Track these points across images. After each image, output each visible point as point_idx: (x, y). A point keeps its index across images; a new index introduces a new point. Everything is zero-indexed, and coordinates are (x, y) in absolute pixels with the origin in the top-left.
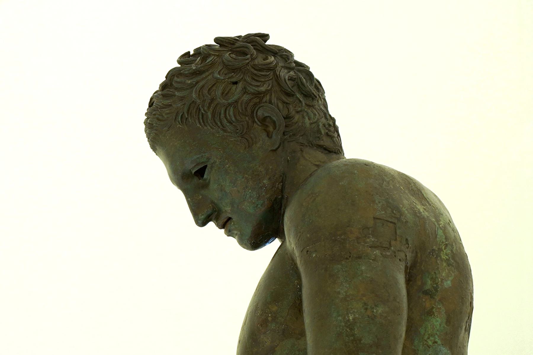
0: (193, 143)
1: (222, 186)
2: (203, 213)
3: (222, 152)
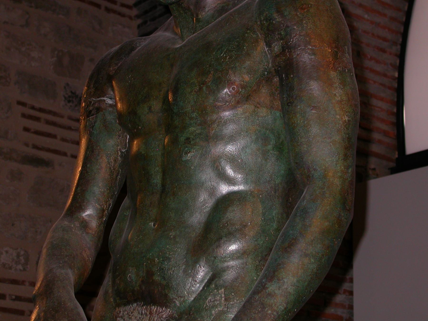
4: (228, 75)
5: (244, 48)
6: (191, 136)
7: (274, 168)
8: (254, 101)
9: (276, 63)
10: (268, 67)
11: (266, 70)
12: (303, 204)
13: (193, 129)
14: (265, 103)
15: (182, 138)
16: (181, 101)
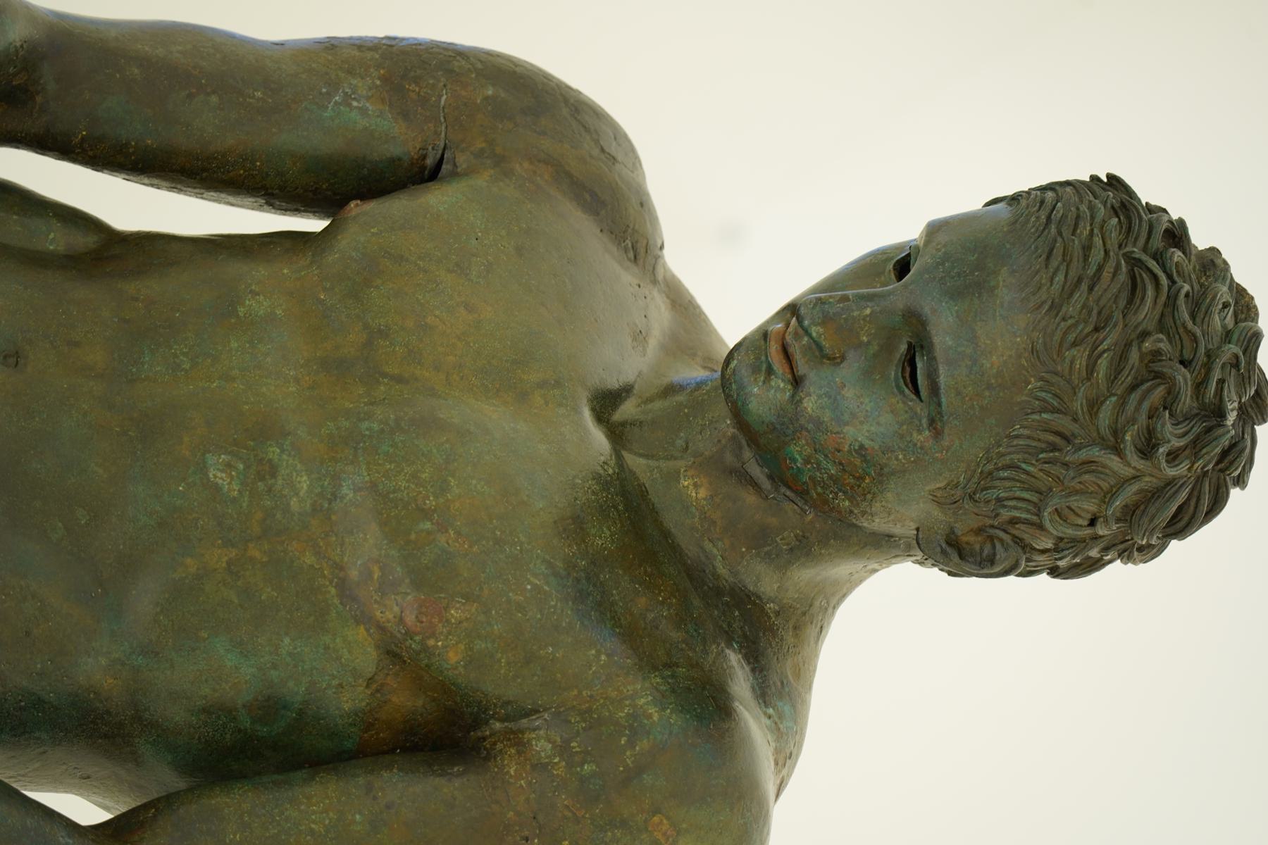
0: (977, 404)
1: (862, 423)
2: (823, 336)
3: (937, 455)
4: (464, 601)
5: (551, 649)
6: (280, 482)
7: (181, 734)
8: (388, 674)
9: (502, 742)
10: (492, 717)
11: (484, 713)
12: (62, 837)
13: (302, 487)
14: (381, 707)
15: (278, 451)
16: (392, 446)
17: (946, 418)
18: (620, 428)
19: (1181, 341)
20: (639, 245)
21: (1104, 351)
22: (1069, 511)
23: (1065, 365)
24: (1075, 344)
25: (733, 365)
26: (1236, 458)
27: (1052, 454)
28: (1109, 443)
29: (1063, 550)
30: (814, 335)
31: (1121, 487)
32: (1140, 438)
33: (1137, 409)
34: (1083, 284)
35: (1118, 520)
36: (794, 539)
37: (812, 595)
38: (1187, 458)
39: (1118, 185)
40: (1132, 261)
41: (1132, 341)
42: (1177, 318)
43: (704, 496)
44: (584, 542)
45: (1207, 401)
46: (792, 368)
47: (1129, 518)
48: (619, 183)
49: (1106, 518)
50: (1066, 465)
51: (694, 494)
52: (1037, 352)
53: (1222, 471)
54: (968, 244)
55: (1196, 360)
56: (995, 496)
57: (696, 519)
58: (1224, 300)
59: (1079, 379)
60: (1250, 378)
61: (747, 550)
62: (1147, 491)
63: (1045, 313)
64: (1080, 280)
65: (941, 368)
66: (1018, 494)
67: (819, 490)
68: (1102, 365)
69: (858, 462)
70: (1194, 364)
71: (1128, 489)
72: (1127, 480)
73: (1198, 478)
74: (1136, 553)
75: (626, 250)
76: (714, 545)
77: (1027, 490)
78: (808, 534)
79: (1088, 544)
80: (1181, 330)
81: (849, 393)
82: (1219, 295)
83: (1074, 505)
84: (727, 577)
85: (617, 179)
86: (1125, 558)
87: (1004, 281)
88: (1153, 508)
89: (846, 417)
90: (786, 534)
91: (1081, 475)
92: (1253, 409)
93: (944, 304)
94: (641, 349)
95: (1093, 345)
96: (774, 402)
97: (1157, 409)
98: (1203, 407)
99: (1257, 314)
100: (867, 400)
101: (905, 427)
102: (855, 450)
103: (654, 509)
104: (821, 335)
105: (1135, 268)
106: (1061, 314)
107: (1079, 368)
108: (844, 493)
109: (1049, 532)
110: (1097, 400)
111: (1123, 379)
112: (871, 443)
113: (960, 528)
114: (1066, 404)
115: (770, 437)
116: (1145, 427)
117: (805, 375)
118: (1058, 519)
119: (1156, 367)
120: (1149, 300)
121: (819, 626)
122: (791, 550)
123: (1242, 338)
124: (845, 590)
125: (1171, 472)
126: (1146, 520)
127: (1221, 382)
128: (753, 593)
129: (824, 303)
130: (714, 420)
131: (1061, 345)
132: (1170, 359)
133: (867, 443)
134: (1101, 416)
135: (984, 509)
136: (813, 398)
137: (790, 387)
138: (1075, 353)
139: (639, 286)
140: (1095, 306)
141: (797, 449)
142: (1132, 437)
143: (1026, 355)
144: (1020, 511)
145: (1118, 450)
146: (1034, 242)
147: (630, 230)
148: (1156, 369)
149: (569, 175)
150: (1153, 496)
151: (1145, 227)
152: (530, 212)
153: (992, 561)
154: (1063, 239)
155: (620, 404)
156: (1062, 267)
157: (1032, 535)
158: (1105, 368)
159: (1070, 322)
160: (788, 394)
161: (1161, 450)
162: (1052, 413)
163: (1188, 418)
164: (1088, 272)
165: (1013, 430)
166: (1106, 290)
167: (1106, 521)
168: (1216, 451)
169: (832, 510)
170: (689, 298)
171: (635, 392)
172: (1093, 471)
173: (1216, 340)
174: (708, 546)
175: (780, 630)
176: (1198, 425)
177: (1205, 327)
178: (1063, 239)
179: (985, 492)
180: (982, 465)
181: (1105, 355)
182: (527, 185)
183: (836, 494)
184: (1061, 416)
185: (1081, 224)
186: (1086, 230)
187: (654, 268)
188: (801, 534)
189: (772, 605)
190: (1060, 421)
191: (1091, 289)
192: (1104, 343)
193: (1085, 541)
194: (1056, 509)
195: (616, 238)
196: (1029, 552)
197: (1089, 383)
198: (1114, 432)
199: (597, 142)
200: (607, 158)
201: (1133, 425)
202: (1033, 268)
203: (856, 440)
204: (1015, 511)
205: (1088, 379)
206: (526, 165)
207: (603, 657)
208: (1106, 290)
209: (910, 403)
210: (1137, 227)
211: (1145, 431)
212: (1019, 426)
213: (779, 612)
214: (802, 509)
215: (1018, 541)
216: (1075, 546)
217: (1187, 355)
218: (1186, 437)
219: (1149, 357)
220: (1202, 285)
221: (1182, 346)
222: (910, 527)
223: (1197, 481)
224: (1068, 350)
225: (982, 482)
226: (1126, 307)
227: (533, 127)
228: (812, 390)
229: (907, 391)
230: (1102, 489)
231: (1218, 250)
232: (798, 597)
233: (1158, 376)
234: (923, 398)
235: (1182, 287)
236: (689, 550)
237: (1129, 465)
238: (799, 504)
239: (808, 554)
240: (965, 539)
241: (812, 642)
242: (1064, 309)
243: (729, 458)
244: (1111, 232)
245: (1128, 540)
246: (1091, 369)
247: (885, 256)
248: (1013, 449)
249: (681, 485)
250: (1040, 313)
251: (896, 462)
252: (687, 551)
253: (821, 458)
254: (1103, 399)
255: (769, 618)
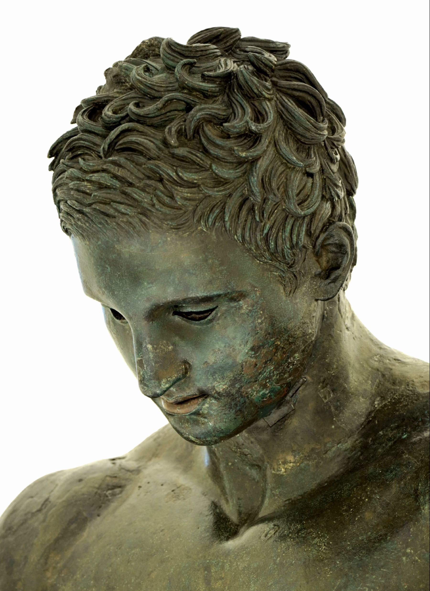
1: (234, 350)
2: (169, 379)
3: (258, 294)
17: (229, 291)
18: (243, 515)
19: (172, 111)
20: (111, 484)
21: (178, 175)
22: (301, 194)
23: (188, 204)
24: (172, 197)
25: (193, 439)
26: (263, 63)
27: (257, 212)
28: (248, 168)
29: (332, 196)
30: (167, 386)
31: (282, 156)
32: (245, 144)
33: (221, 148)
34: (126, 191)
35: (308, 155)
36: (326, 389)
37: (370, 369)
38: (261, 104)
39: (57, 148)
40: (111, 149)
41: (170, 153)
42: (153, 115)
43: (292, 457)
44: (322, 560)
45: (218, 89)
46: (194, 399)
47: (307, 146)
48: (64, 499)
49: (306, 166)
50: (265, 200)
51: (291, 464)
52: (178, 225)
53: (273, 71)
54: (99, 270)
55: (186, 100)
56: (289, 251)
57: (310, 463)
58: (142, 72)
59: (199, 194)
60: (202, 51)
61: (333, 424)
62: (286, 134)
63: (147, 218)
64: (124, 193)
65: (191, 296)
66: (287, 234)
67: (286, 375)
68: (188, 176)
69: (264, 351)
70: (189, 101)
71: (284, 150)
72: (277, 151)
73: (278, 90)
74: (336, 136)
75: (114, 495)
76: (330, 450)
77: (284, 227)
78: (322, 379)
79: (327, 177)
80: (163, 111)
81: (211, 359)
82: (138, 77)
83: (296, 191)
84: (354, 440)
85: (60, 501)
86: (339, 143)
87: (125, 248)
88: (299, 130)
89: (230, 361)
90: (321, 396)
91: (272, 190)
92: (227, 42)
93: (143, 293)
94: (185, 491)
95: (173, 184)
96: (220, 411)
97: (222, 131)
98: (222, 91)
99: (156, 39)
100: (217, 347)
101: (237, 319)
102: (255, 354)
103: (302, 495)
104: (168, 381)
105: (116, 148)
106: (150, 208)
107: (191, 193)
108: (289, 357)
109: (317, 208)
110: (215, 179)
111: (199, 160)
112: (249, 343)
113: (316, 269)
114: (218, 203)
115: (246, 413)
116: (236, 141)
117: (199, 390)
118: (306, 203)
119: (190, 133)
120: (140, 139)
121: (393, 362)
122: (333, 390)
123: (172, 58)
124: (368, 341)
125: (271, 116)
126: (308, 135)
127: (204, 78)
128: (367, 418)
129: (144, 378)
130: (236, 445)
131: (173, 208)
132: (185, 121)
133: (249, 346)
134: (227, 176)
135: (300, 256)
136: (216, 384)
137: (208, 400)
138: (179, 197)
139: (140, 487)
140: (144, 181)
141: (255, 394)
142: (244, 151)
143: (180, 233)
144: (301, 232)
145: (254, 161)
146: (96, 225)
147: (99, 491)
148: (191, 133)
149: (57, 540)
150: (290, 129)
151: (86, 136)
152: (83, 576)
153: (341, 246)
154: (94, 203)
155: (225, 514)
156: (115, 206)
157: (320, 220)
158: (191, 174)
159: (155, 201)
160: (213, 401)
161: (253, 128)
162: (224, 213)
163: (230, 105)
164: (118, 186)
165: (239, 240)
166: (132, 173)
167: (309, 166)
168: (256, 82)
169: (302, 364)
170: (152, 440)
171: (216, 500)
172: (270, 179)
173: (172, 79)
174: (330, 454)
175: (395, 396)
176: (236, 96)
177: (162, 89)
178: (94, 203)
179: (287, 257)
180: (266, 260)
181: (180, 174)
182: (63, 575)
183: (289, 363)
184: (227, 207)
185: (83, 188)
186: (86, 185)
187: (128, 471)
188: (321, 384)
189: (376, 403)
190: (231, 207)
191: (131, 185)
192: (171, 175)
193: (325, 179)
194: (298, 205)
195: (104, 503)
196: (334, 218)
197: (202, 186)
198: (239, 165)
199: (33, 514)
200: (45, 508)
201: (234, 151)
202: (116, 227)
203: (247, 353)
204: (301, 235)
205: (199, 186)
206: (49, 574)
207: (408, 551)
208: (132, 173)
209: (219, 315)
210: (86, 143)
211: (239, 140)
212: (235, 236)
213: (381, 397)
214: (302, 384)
215: (325, 228)
216: (328, 187)
217: (182, 106)
218: (244, 107)
219: (183, 138)
220: (132, 88)
221: (176, 110)
222: (315, 306)
223: (281, 91)
224: (176, 202)
225: (279, 259)
226: (145, 156)
227: (21, 566)
228: (209, 385)
229: (209, 317)
230: (284, 171)
231: (107, 70)
232: (371, 381)
233: (197, 130)
234: (215, 306)
235: (130, 110)
236: (333, 469)
237: (265, 151)
238: (299, 385)
239: (337, 378)
240: (324, 264)
241: (405, 369)
242: (146, 205)
243: (265, 436)
244: (89, 165)
245: (325, 144)
246: (191, 185)
247: (111, 323)
248: (253, 240)
249: (285, 474)
250: (148, 223)
251: (264, 324)
252: (334, 472)
253: (262, 377)
254: (214, 175)
255: (385, 405)
